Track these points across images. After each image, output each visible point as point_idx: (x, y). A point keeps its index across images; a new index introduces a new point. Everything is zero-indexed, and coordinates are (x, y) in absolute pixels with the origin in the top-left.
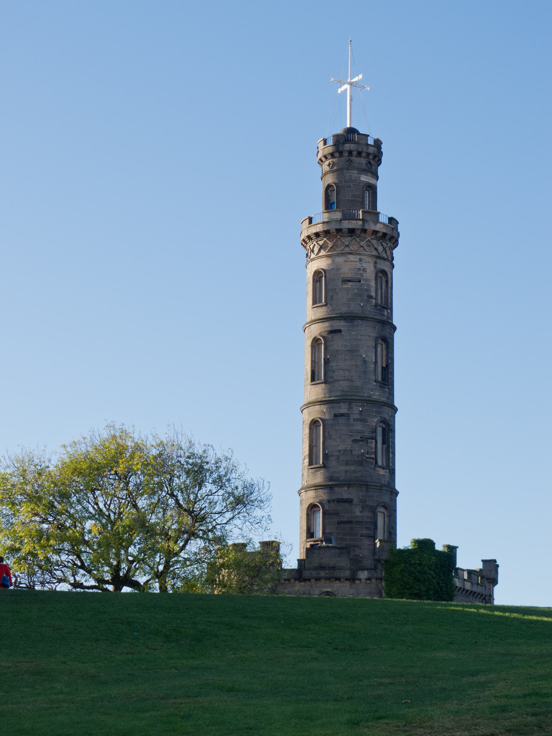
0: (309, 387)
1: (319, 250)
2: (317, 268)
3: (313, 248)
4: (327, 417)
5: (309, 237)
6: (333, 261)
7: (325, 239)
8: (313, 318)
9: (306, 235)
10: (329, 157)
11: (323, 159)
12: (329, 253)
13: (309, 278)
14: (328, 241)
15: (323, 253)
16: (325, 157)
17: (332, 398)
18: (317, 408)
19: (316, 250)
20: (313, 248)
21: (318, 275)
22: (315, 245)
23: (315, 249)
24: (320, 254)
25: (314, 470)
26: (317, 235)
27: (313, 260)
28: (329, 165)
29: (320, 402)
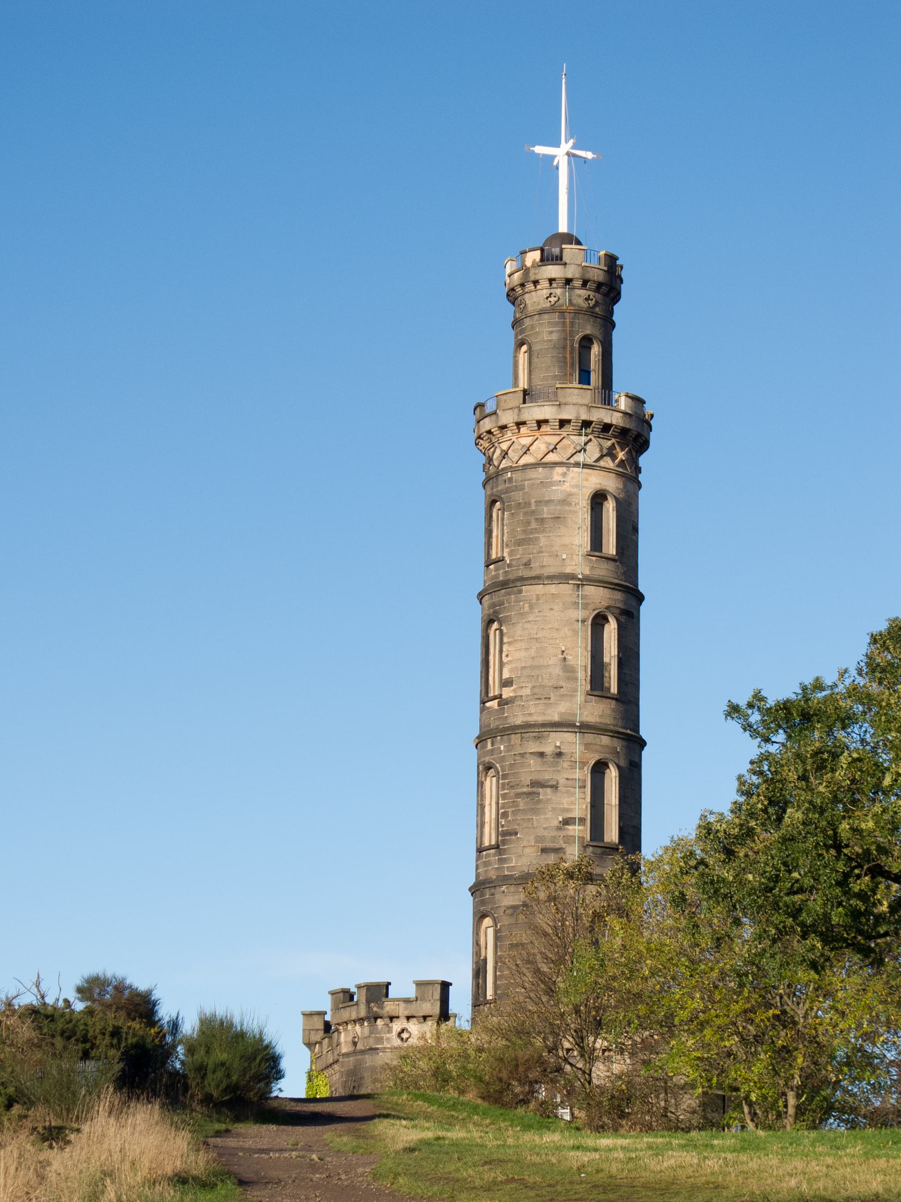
0: (580, 697)
1: (602, 457)
2: (598, 487)
3: (586, 444)
4: (622, 763)
5: (586, 424)
6: (625, 486)
7: (613, 440)
8: (587, 572)
9: (584, 417)
10: (594, 286)
11: (578, 283)
12: (620, 470)
13: (570, 495)
14: (617, 447)
15: (607, 462)
16: (585, 283)
17: (628, 731)
18: (605, 740)
19: (593, 452)
20: (586, 444)
21: (598, 499)
22: (590, 440)
23: (588, 447)
24: (602, 463)
25: (599, 851)
26: (606, 427)
27: (586, 466)
28: (588, 299)
29: (612, 731)
